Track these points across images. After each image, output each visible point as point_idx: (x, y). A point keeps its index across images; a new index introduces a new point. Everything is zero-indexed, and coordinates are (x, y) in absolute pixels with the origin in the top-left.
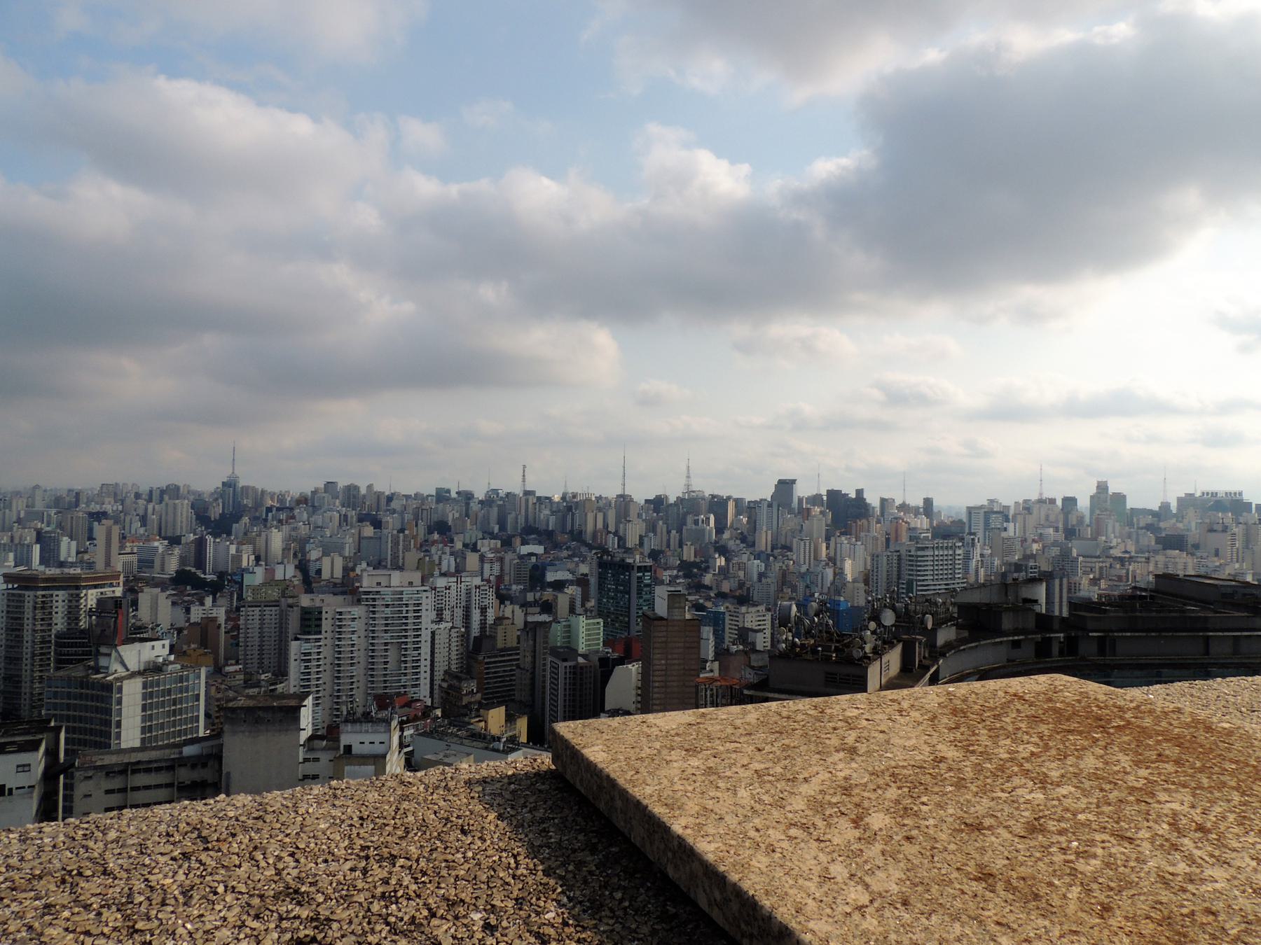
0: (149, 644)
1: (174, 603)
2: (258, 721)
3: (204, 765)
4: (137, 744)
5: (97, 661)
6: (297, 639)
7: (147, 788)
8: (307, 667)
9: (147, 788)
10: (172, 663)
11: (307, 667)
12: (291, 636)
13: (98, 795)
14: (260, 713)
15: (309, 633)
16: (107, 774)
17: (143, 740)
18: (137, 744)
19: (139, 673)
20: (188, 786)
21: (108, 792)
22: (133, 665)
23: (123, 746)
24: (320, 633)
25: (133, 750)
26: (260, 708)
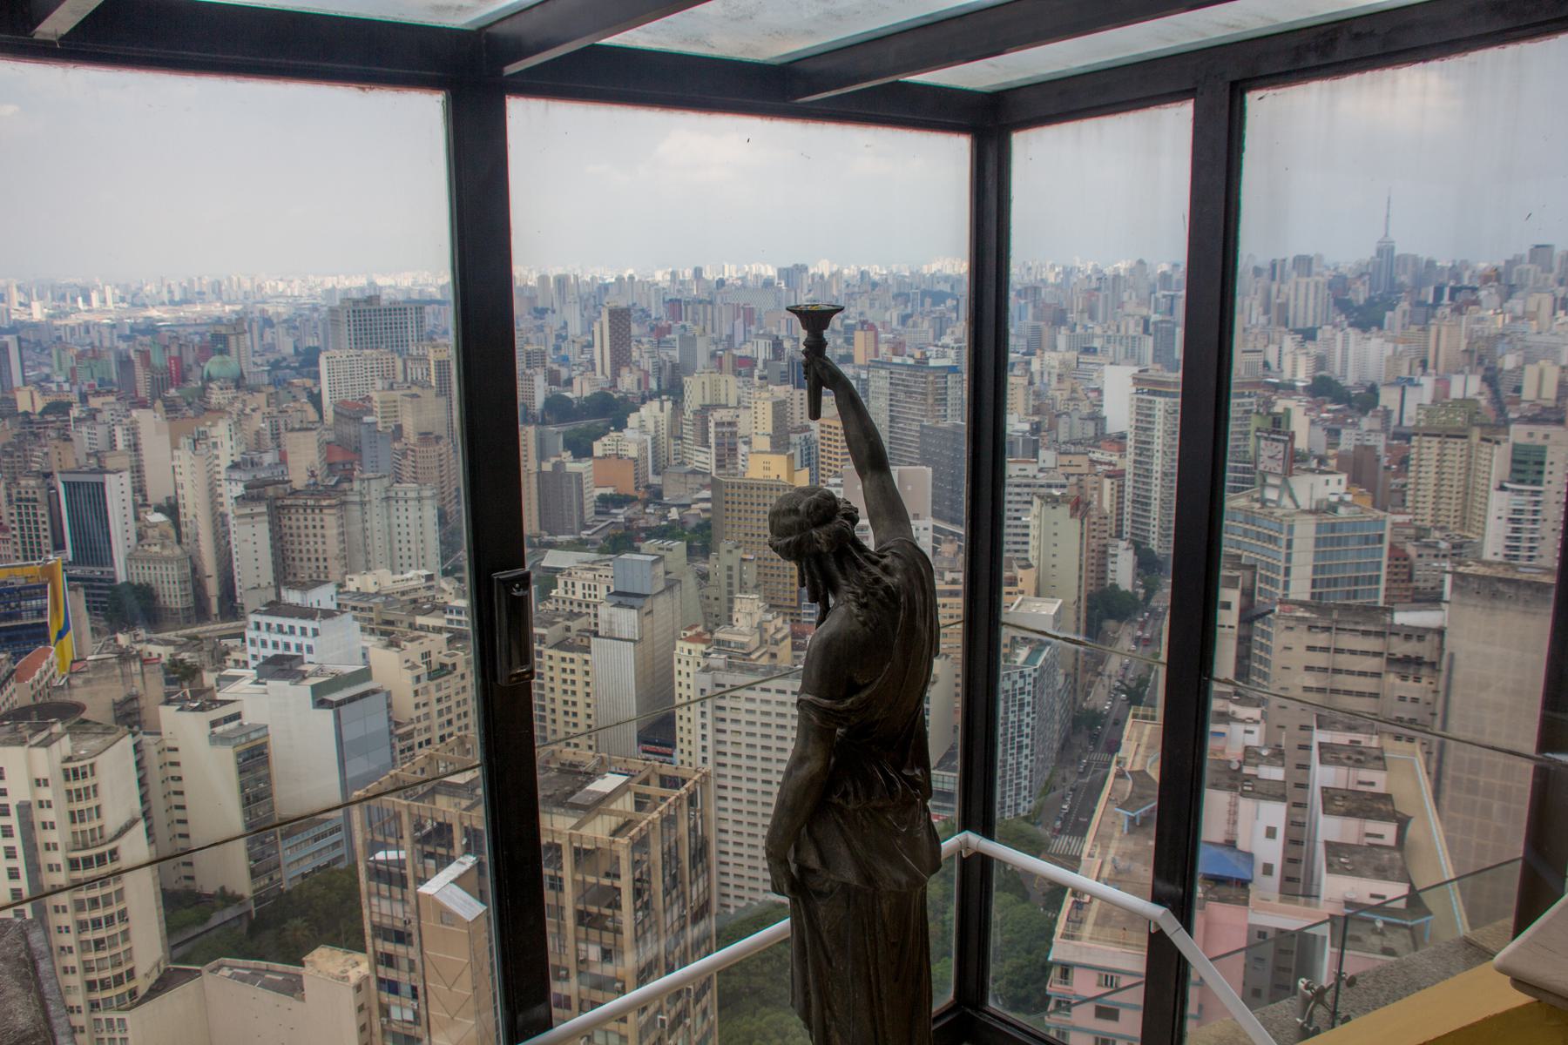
0: (1324, 478)
1: (1313, 422)
2: (1495, 595)
3: (1421, 638)
4: (1306, 597)
5: (1262, 492)
6: (1502, 488)
7: (1353, 652)
8: (1516, 530)
9: (1353, 652)
10: (1347, 504)
11: (1516, 530)
12: (1494, 483)
13: (1299, 649)
14: (1500, 587)
15: (1521, 482)
16: (1310, 628)
17: (1313, 595)
18: (1306, 597)
19: (1310, 512)
20: (1399, 660)
21: (1310, 648)
22: (1305, 503)
23: (1292, 597)
24: (1539, 483)
25: (1302, 604)
26: (1500, 580)
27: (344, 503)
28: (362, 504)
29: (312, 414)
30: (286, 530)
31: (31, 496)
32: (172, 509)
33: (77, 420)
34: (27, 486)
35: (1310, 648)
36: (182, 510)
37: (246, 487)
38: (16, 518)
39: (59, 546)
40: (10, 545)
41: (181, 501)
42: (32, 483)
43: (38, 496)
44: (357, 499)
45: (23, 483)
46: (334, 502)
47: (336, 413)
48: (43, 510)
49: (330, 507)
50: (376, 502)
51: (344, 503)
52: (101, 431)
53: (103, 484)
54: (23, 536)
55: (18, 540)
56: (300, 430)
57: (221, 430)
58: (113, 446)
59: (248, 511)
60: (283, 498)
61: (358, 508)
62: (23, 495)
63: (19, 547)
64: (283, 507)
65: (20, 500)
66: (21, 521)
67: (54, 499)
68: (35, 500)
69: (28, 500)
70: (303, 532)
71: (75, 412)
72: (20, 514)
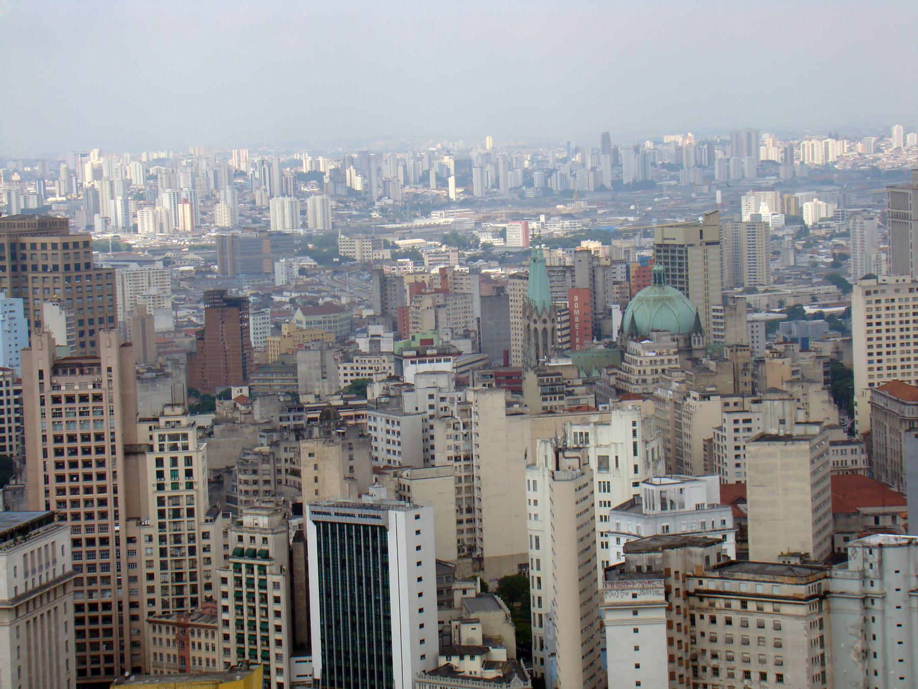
27: (824, 596)
28: (866, 599)
29: (820, 405)
30: (703, 643)
31: (258, 546)
32: (516, 592)
33: (378, 406)
34: (254, 528)
35: (66, 612)
36: (534, 592)
37: (629, 549)
38: (230, 588)
39: (300, 647)
40: (218, 640)
41: (533, 573)
42: (263, 521)
43: (270, 547)
44: (854, 587)
45: (247, 520)
46: (802, 590)
47: (874, 406)
48: (275, 577)
49: (795, 600)
50: (895, 598)
51: (824, 596)
52: (409, 426)
53: (384, 530)
54: (239, 624)
55: (232, 631)
56: (775, 438)
57: (616, 435)
58: (428, 460)
59: (628, 599)
60: (700, 578)
61: (856, 606)
62: (246, 545)
63: (232, 644)
64: (701, 594)
65: (240, 553)
66: (238, 597)
67: (299, 556)
68: (265, 555)
69: (253, 554)
70: (737, 649)
71: (375, 391)
72: (238, 581)
